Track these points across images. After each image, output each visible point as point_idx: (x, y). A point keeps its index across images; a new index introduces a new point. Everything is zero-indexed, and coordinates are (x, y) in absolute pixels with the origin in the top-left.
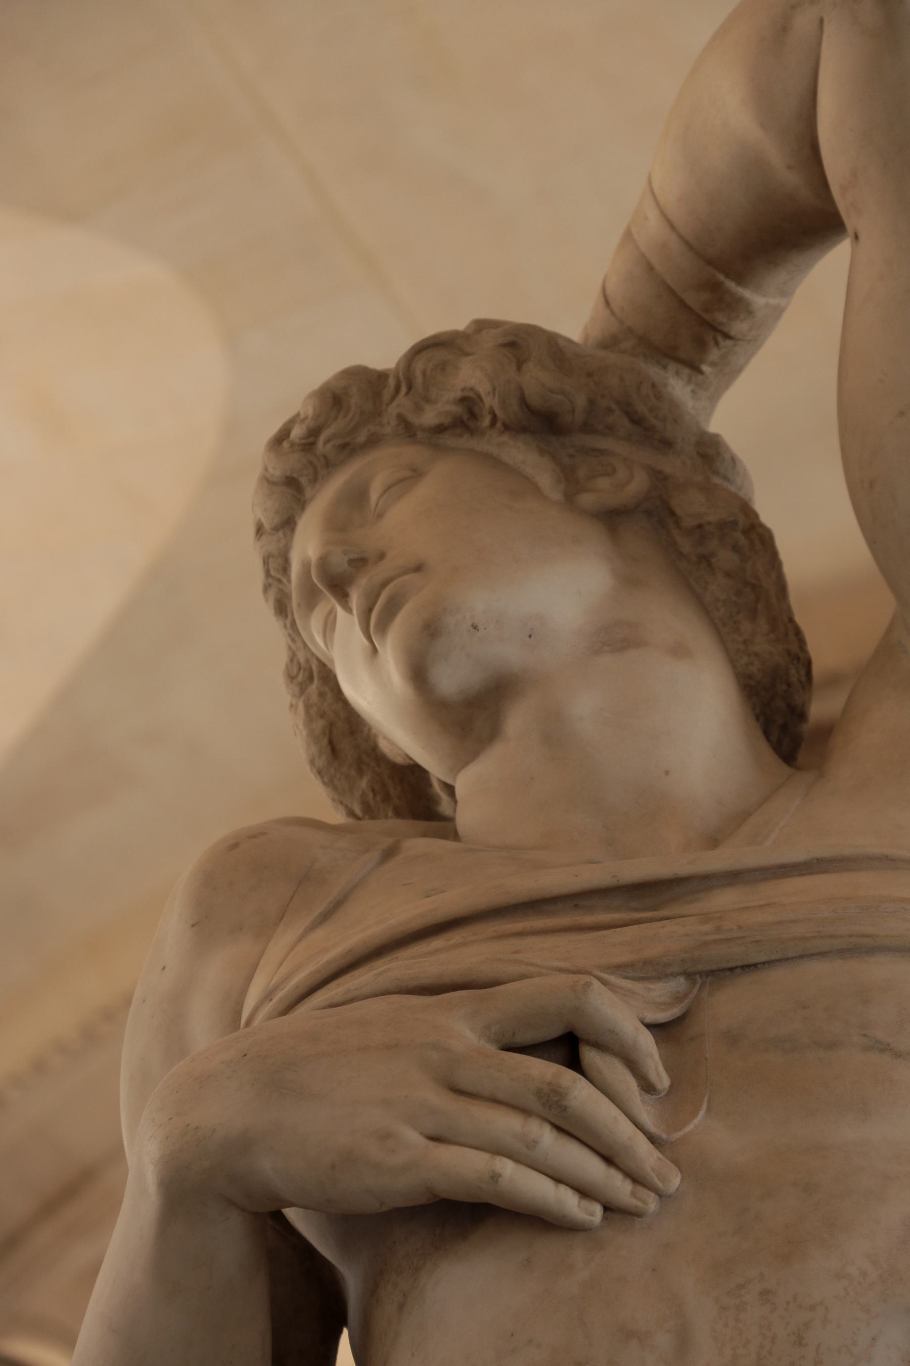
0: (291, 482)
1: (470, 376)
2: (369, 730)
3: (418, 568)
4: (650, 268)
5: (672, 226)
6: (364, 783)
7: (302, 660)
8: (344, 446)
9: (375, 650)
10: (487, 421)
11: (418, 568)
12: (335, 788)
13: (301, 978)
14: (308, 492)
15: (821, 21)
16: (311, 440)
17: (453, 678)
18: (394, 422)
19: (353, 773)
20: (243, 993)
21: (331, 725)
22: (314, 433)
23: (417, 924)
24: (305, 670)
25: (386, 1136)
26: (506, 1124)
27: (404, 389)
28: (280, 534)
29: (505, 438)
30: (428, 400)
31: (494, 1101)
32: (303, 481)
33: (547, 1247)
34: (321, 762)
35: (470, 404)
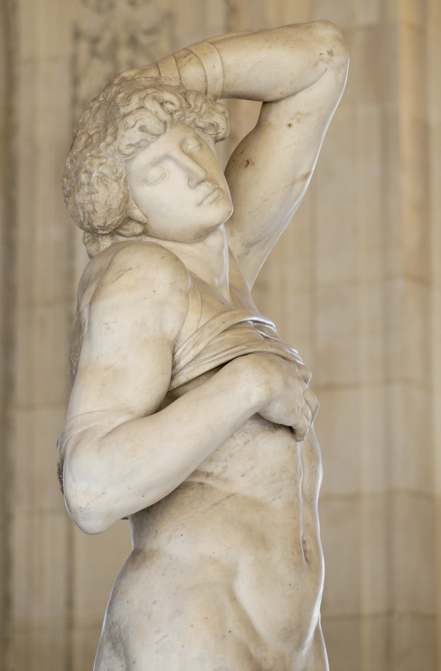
0: (165, 123)
2: (132, 204)
4: (206, 81)
5: (224, 77)
6: (118, 218)
7: (120, 169)
8: (179, 119)
10: (211, 133)
14: (168, 130)
15: (326, 69)
16: (174, 112)
18: (192, 119)
20: (186, 315)
21: (124, 197)
22: (176, 111)
24: (120, 173)
28: (154, 137)
29: (211, 140)
32: (169, 125)
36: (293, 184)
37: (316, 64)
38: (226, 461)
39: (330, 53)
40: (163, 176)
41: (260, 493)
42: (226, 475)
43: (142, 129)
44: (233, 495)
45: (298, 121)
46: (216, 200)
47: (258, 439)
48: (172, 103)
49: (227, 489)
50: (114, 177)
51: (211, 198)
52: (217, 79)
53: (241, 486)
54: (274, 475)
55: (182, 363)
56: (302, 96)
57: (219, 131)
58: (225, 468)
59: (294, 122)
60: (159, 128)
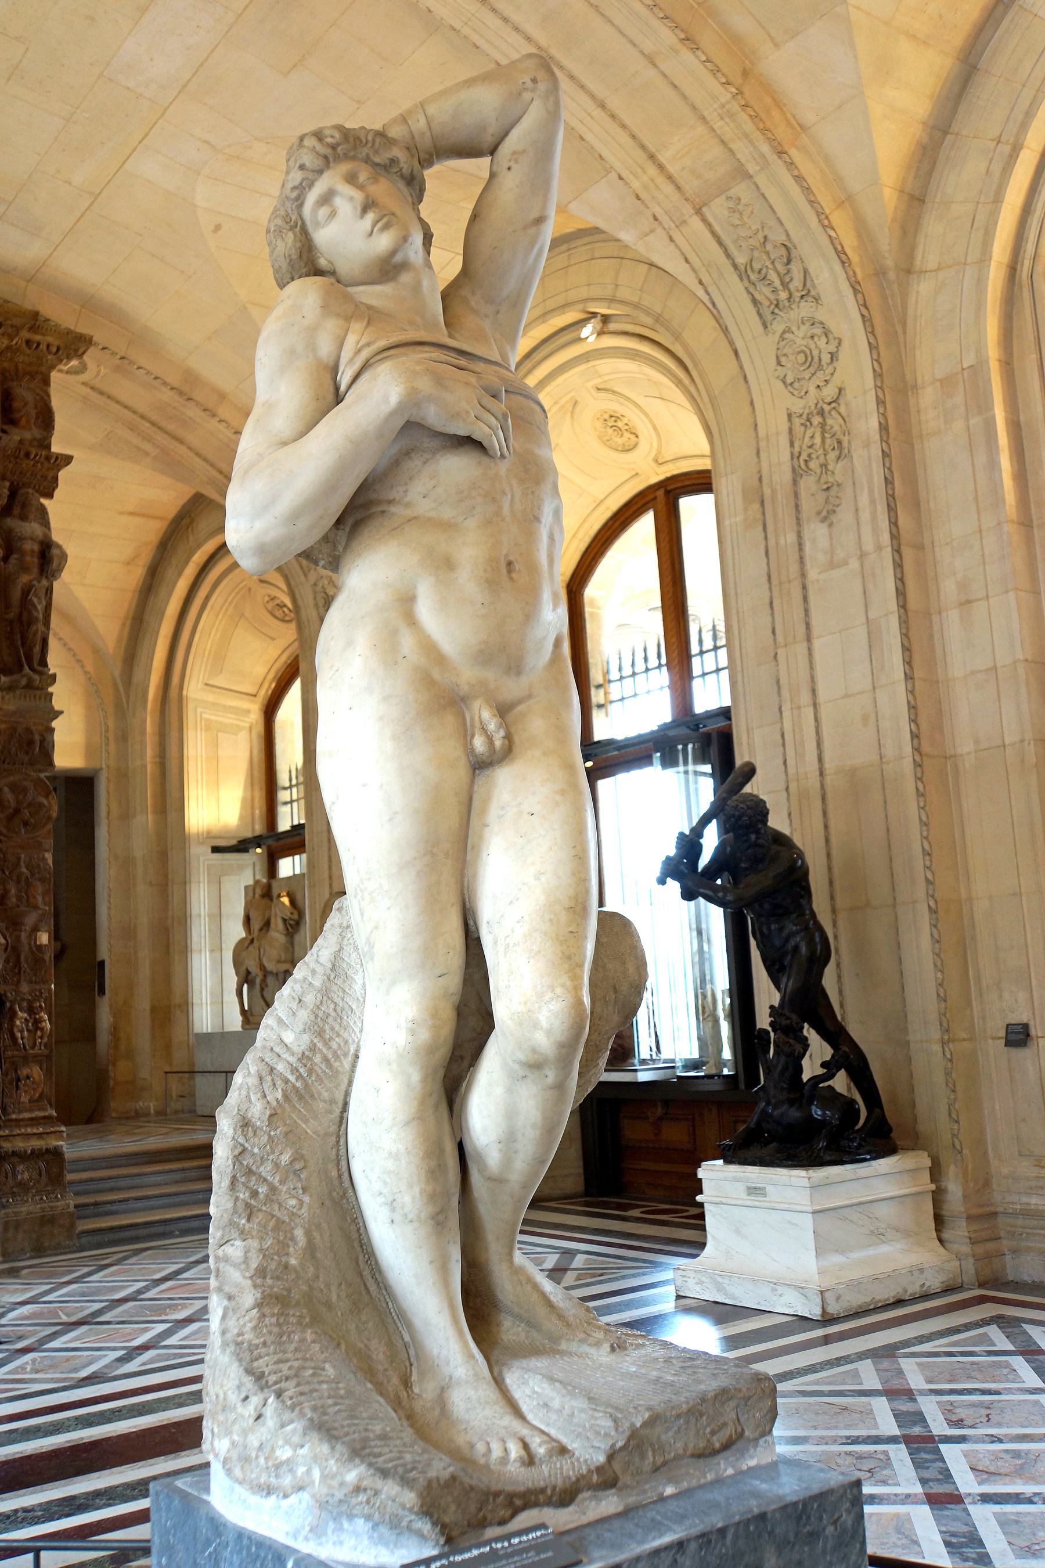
1: (398, 153)
3: (393, 214)
4: (413, 137)
7: (294, 218)
9: (371, 234)
11: (393, 214)
12: (293, 267)
13: (382, 343)
14: (331, 165)
17: (398, 258)
19: (303, 265)
23: (418, 339)
25: (467, 412)
26: (493, 420)
27: (370, 145)
30: (377, 152)
31: (489, 411)
32: (331, 160)
33: (485, 460)
34: (294, 257)
35: (393, 161)
36: (525, 228)
37: (520, 94)
38: (406, 484)
39: (534, 81)
40: (333, 214)
41: (447, 513)
42: (407, 500)
43: (302, 167)
44: (415, 518)
45: (516, 161)
46: (386, 227)
47: (438, 456)
48: (332, 137)
49: (409, 513)
50: (288, 227)
51: (379, 225)
52: (424, 133)
53: (424, 507)
54: (462, 492)
55: (343, 388)
56: (515, 134)
57: (402, 165)
58: (406, 491)
59: (512, 164)
60: (318, 163)
